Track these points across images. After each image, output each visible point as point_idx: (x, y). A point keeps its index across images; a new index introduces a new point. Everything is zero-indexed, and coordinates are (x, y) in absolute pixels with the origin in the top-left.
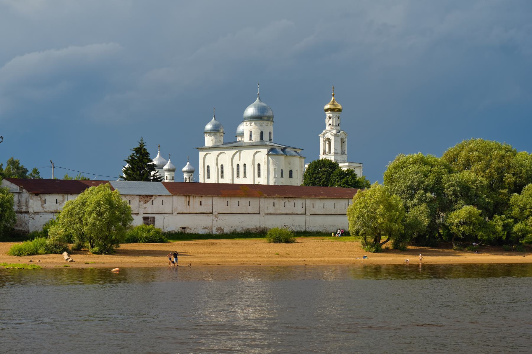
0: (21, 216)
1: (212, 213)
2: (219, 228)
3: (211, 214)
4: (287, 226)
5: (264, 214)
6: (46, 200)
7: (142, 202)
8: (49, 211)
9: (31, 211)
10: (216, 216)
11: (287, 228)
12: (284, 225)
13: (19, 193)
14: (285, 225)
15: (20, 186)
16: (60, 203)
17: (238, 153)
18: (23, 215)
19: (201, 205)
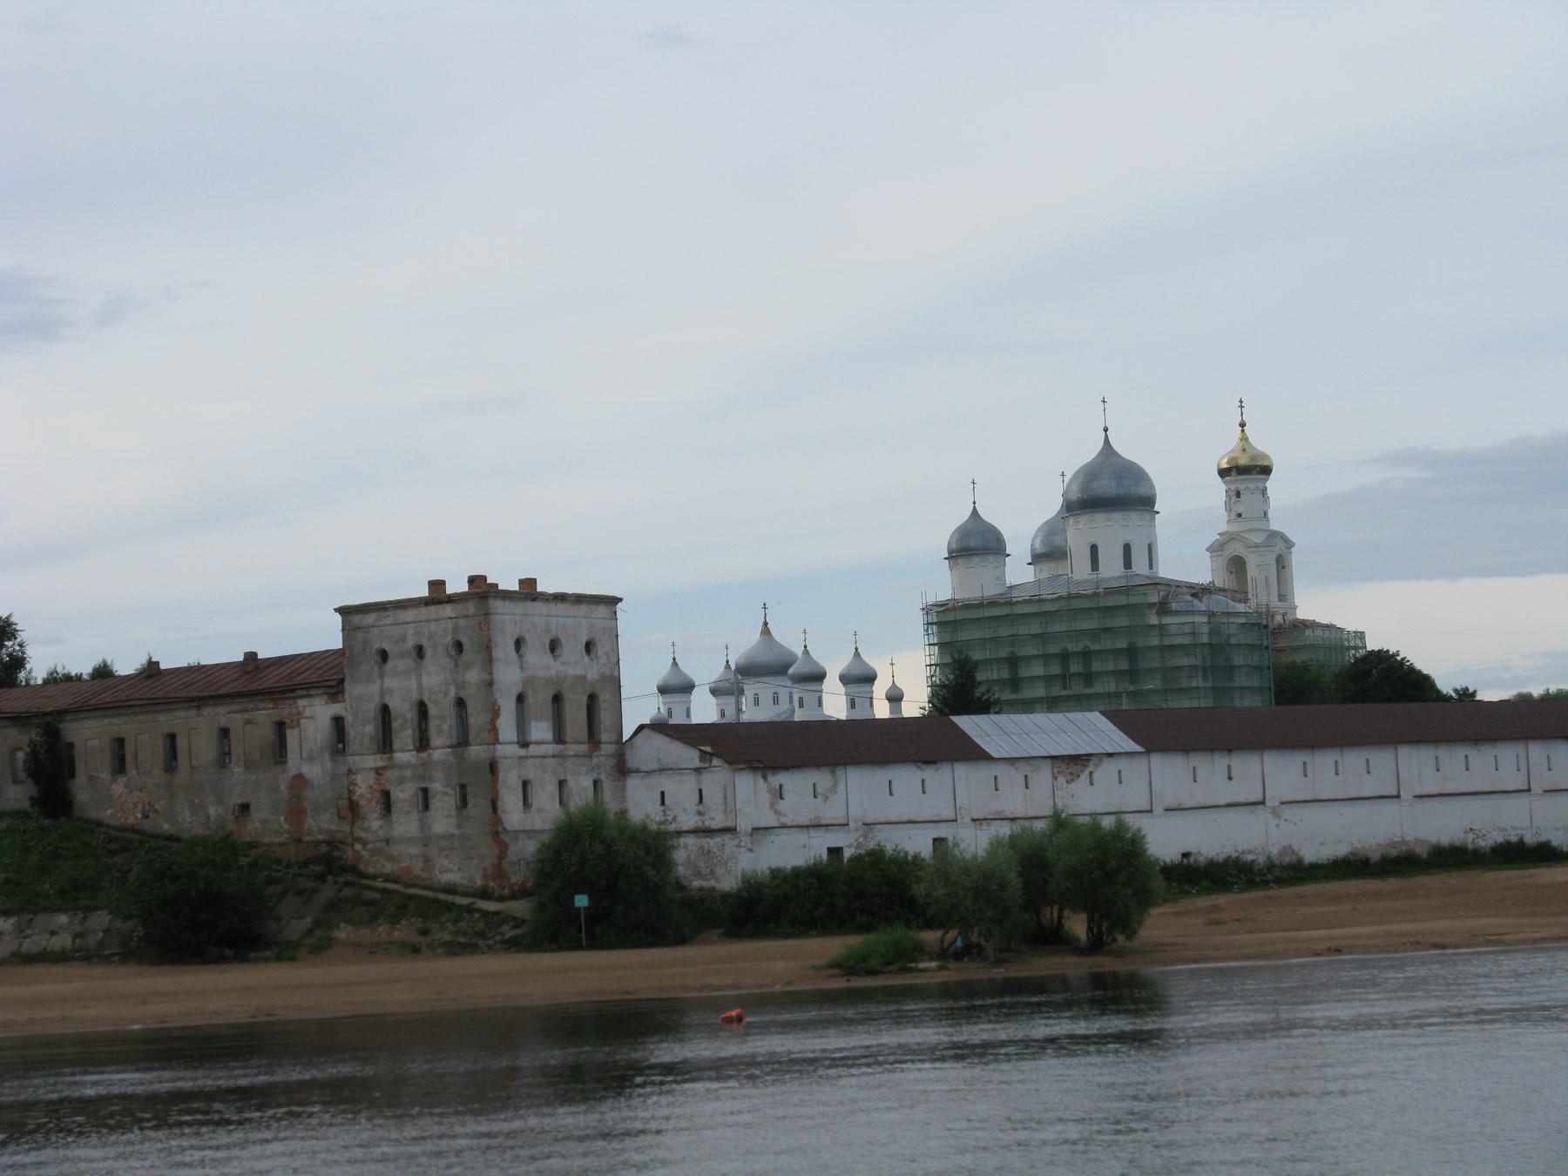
0: (712, 842)
1: (1263, 803)
2: (1285, 848)
3: (1261, 807)
4: (1479, 831)
5: (1410, 797)
6: (785, 788)
7: (1061, 780)
8: (795, 824)
9: (744, 824)
10: (1275, 813)
11: (1478, 837)
12: (1471, 829)
13: (698, 770)
14: (1474, 827)
15: (702, 748)
16: (824, 795)
18: (719, 840)
19: (1195, 781)
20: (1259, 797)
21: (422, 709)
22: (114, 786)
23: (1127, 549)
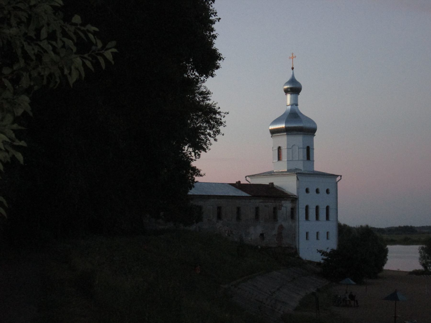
22: (217, 224)
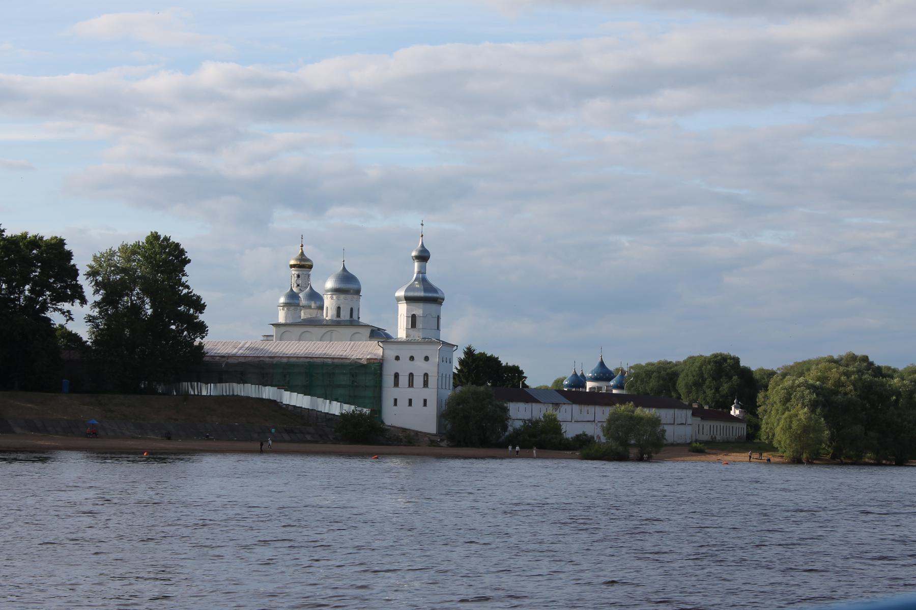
1: (594, 421)
7: (554, 410)
17: (330, 332)
20: (593, 419)
21: (411, 375)
23: (352, 309)
